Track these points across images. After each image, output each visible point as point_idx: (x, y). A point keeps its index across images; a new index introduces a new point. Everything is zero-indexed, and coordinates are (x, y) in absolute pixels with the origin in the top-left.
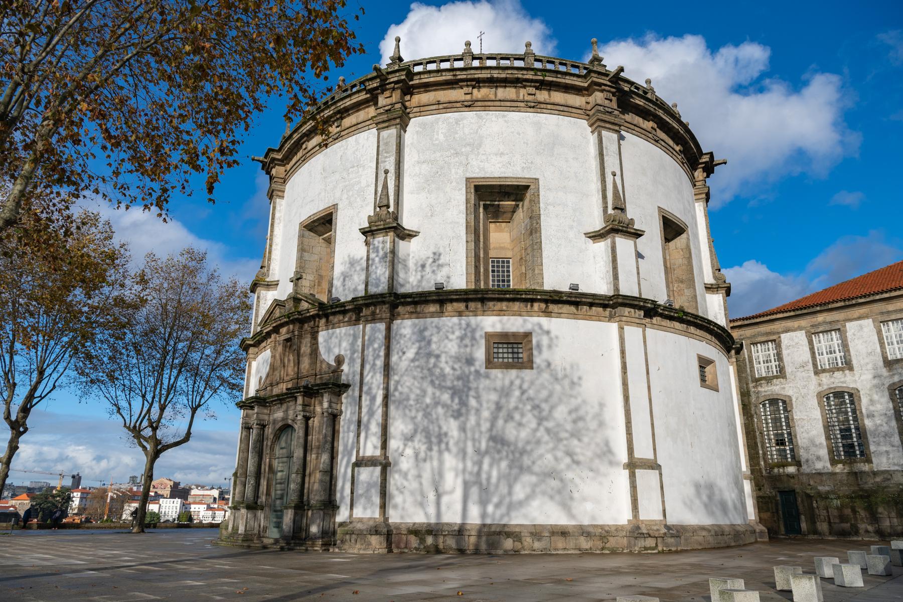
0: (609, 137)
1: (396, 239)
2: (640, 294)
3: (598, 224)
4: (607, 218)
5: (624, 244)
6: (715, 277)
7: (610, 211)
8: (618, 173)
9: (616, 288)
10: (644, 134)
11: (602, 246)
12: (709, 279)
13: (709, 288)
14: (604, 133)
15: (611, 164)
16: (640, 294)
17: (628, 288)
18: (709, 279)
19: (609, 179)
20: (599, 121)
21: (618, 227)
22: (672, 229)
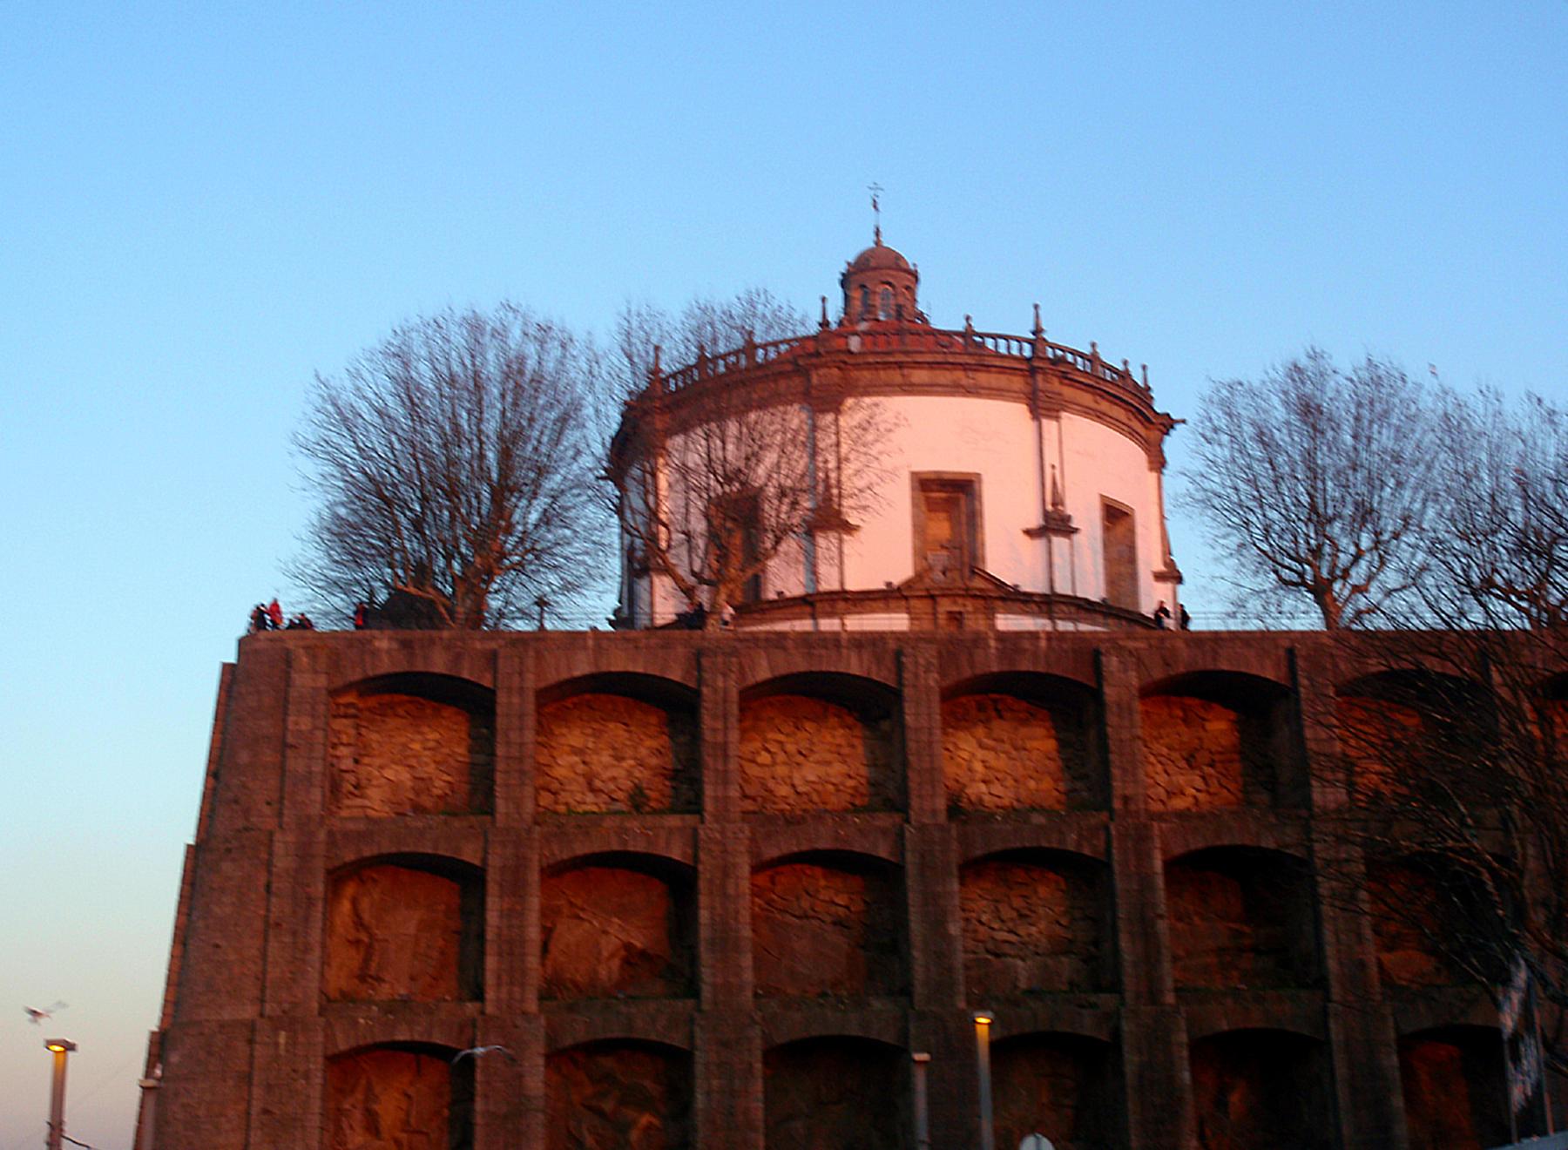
0: (1049, 425)
1: (845, 537)
2: (1074, 589)
3: (1035, 521)
4: (1046, 514)
5: (1059, 542)
6: (1166, 564)
7: (1049, 508)
8: (1057, 465)
9: (1052, 587)
10: (1087, 412)
11: (1039, 544)
12: (1160, 567)
13: (1159, 577)
14: (1045, 422)
15: (1051, 457)
16: (1074, 589)
17: (1063, 588)
18: (1160, 567)
19: (1048, 470)
20: (1042, 407)
21: (1055, 524)
22: (1115, 515)
